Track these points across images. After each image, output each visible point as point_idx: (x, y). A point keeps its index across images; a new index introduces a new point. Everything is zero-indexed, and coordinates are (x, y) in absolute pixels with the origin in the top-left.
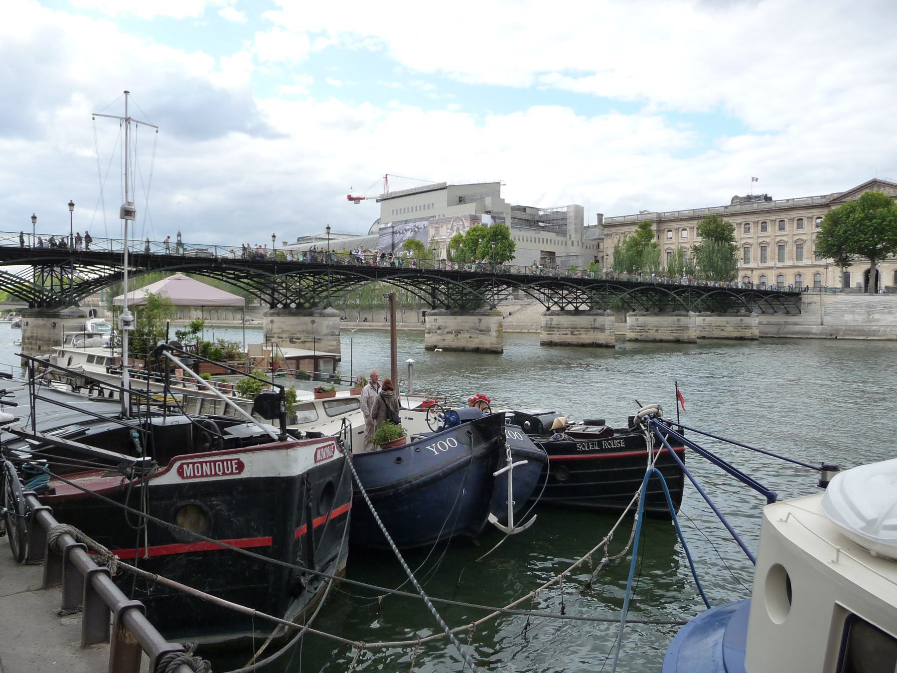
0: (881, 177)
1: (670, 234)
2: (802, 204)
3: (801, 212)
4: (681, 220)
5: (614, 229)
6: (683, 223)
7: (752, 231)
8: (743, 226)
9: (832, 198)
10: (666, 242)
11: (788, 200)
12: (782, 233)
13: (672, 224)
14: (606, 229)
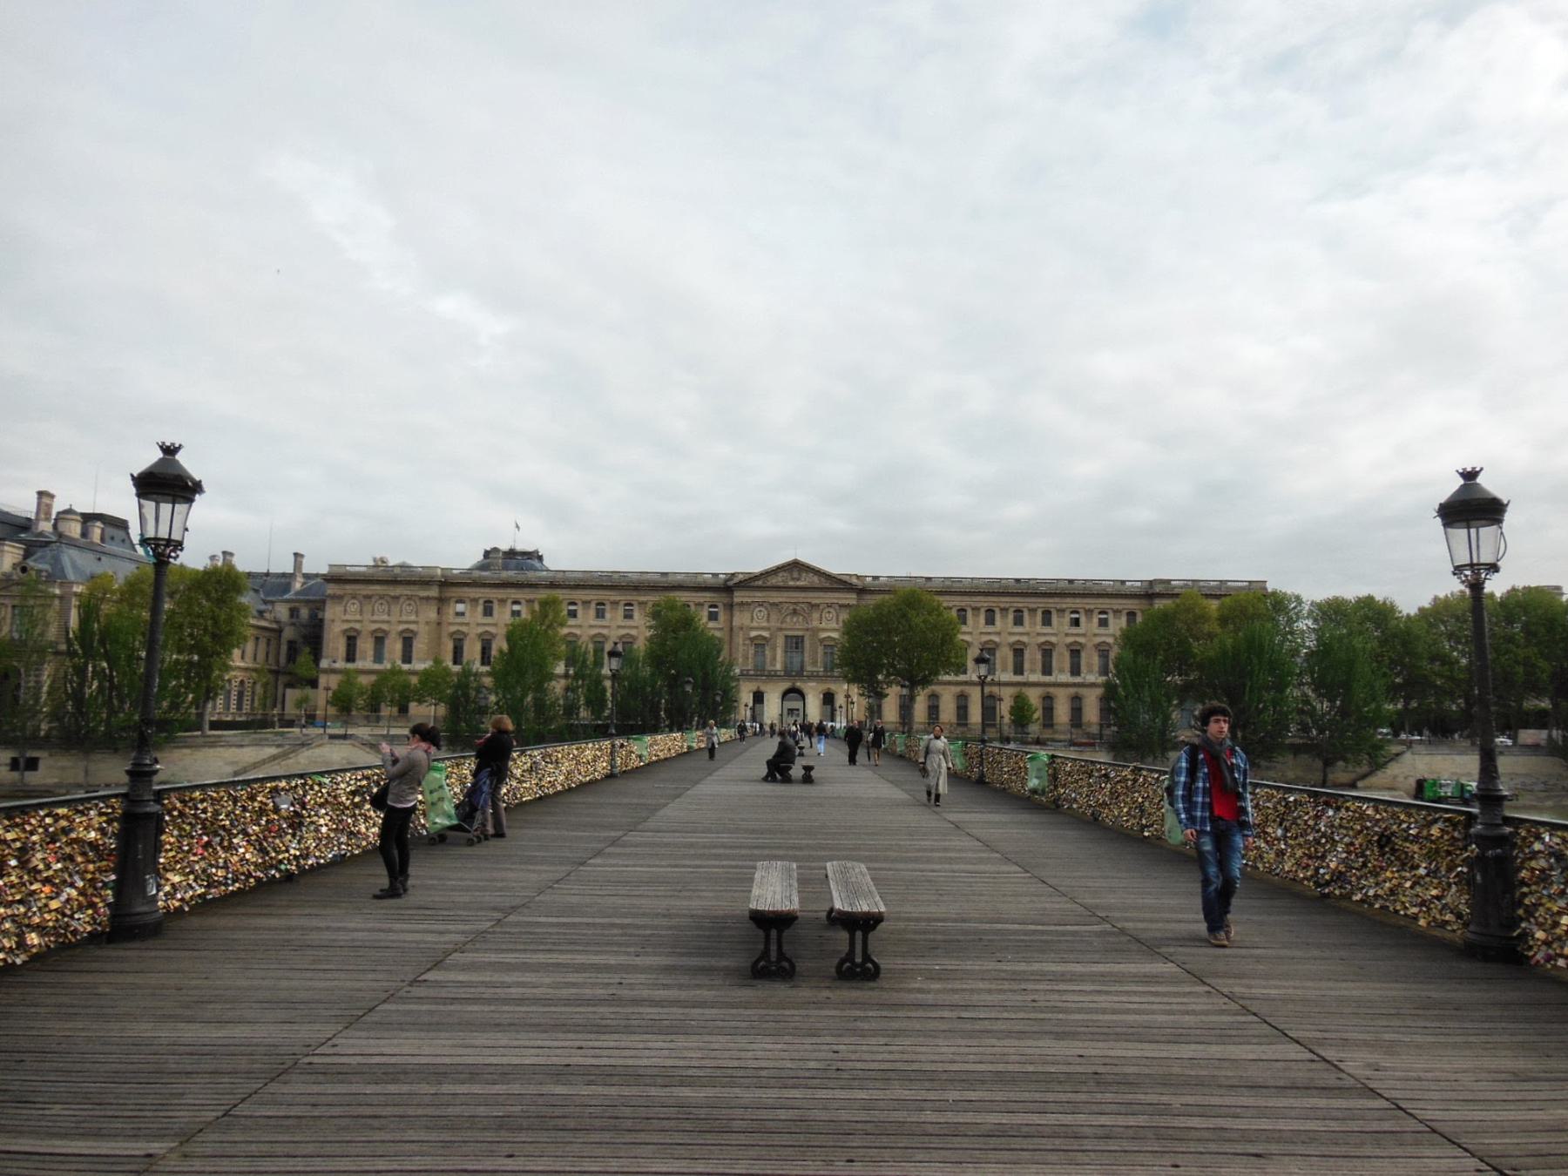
0: (805, 558)
1: (460, 607)
2: (689, 581)
3: (686, 594)
4: (484, 585)
5: (349, 588)
6: (487, 590)
7: (608, 615)
8: (593, 605)
9: (736, 580)
10: (451, 618)
11: (664, 574)
12: (629, 623)
13: (466, 589)
14: (331, 586)
